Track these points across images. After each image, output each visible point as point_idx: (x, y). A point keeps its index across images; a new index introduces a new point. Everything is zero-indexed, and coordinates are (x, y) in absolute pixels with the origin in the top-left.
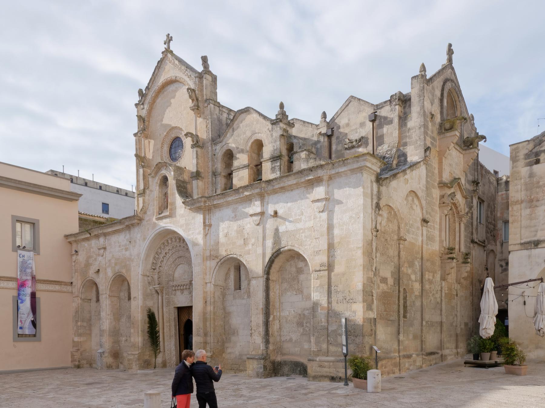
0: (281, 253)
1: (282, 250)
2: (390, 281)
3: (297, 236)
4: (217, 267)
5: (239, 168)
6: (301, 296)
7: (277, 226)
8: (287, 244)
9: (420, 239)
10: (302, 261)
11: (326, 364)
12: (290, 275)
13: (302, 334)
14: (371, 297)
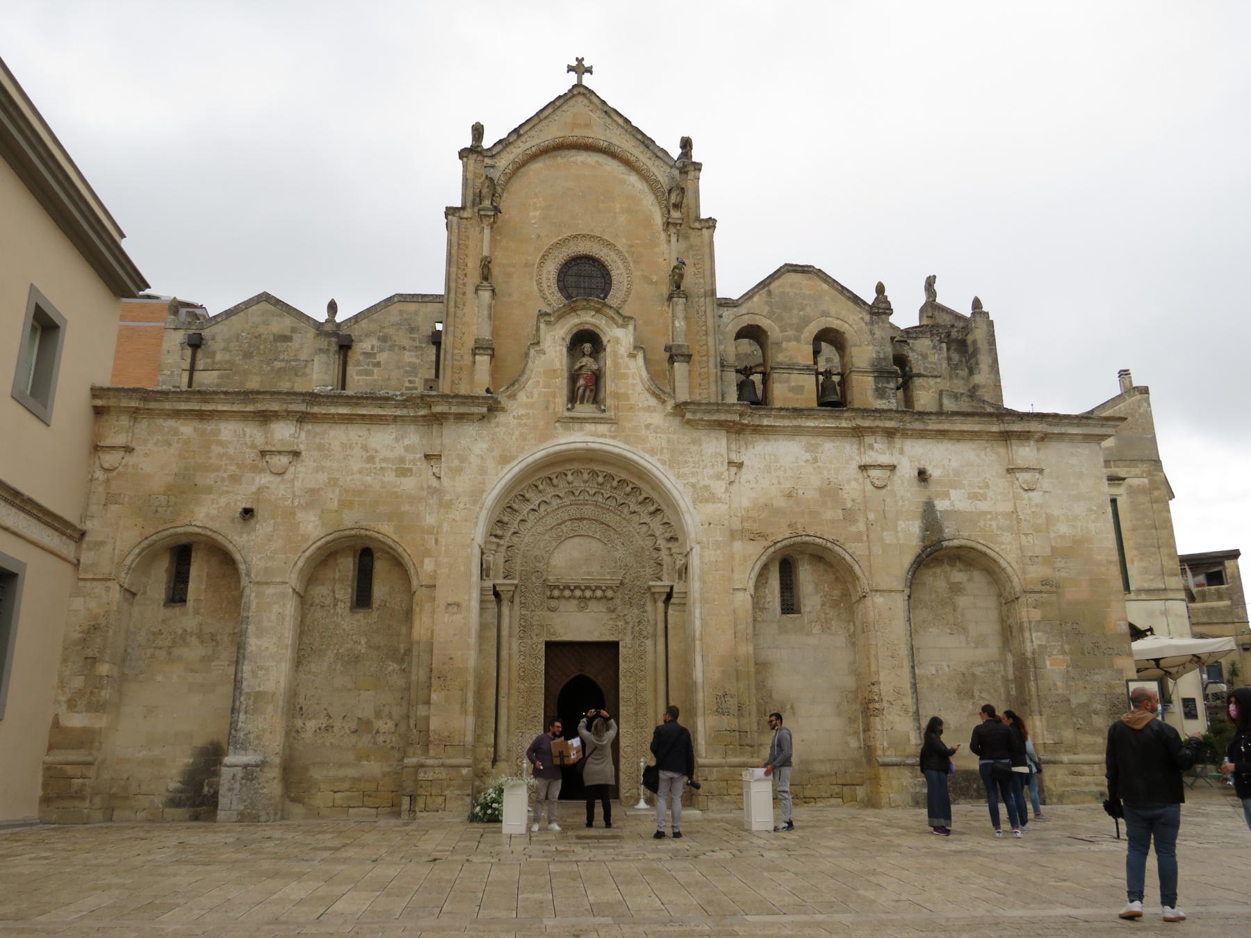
1: (945, 544)
3: (981, 524)
5: (791, 367)
8: (955, 535)
11: (1085, 767)
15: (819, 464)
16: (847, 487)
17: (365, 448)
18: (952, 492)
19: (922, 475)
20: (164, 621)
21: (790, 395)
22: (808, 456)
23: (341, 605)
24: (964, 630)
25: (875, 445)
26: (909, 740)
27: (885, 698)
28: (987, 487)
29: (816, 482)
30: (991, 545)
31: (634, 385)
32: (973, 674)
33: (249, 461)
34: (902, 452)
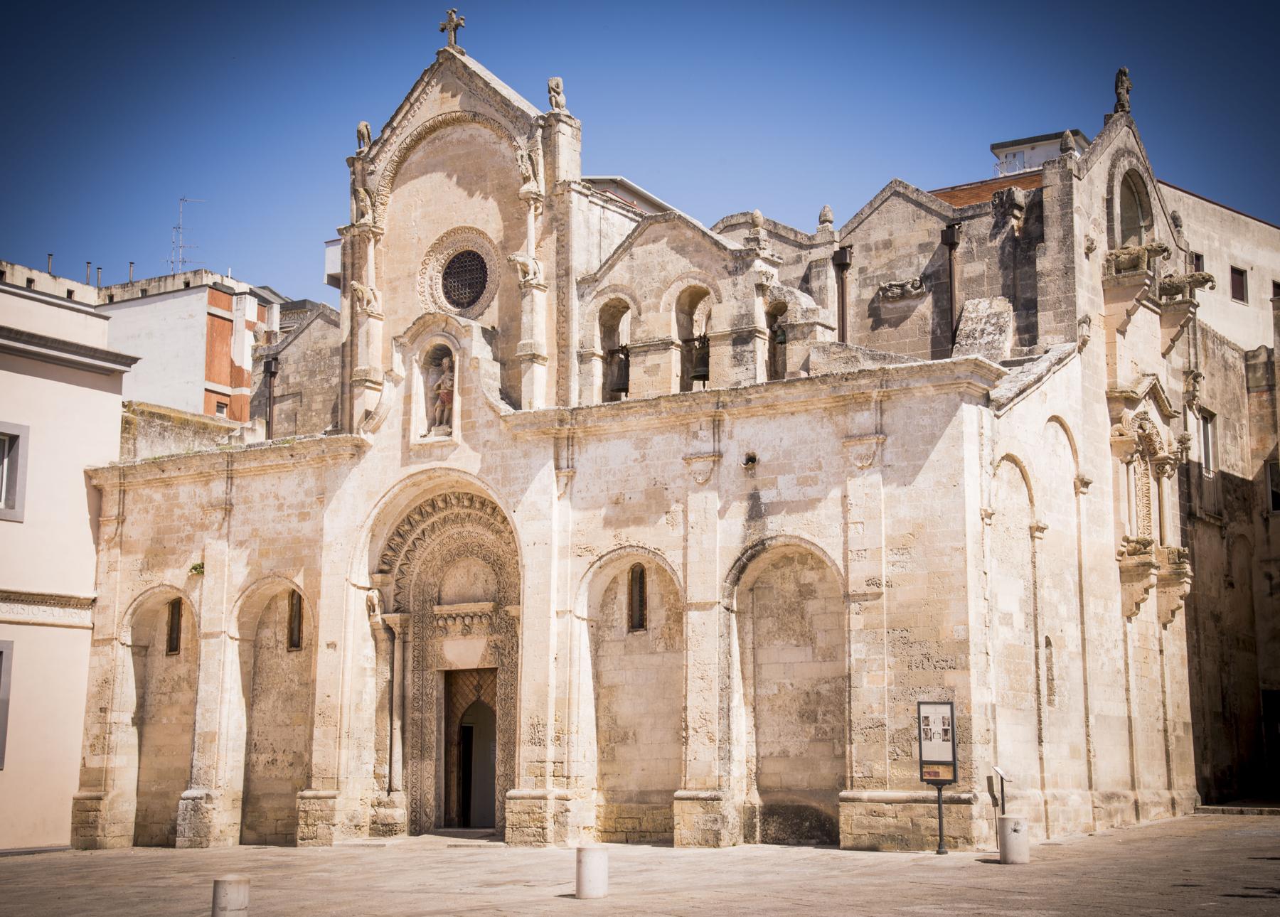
0: (764, 549)
2: (1019, 620)
4: (590, 575)
6: (809, 650)
7: (756, 489)
9: (1074, 521)
10: (812, 569)
12: (781, 601)
13: (814, 740)
14: (984, 656)
15: (648, 462)
16: (672, 485)
17: (277, 497)
18: (782, 480)
19: (751, 460)
20: (166, 670)
21: (646, 377)
22: (637, 454)
23: (281, 646)
24: (812, 640)
25: (700, 433)
26: (710, 771)
27: (691, 725)
28: (820, 468)
29: (642, 483)
30: (816, 540)
31: (476, 399)
32: (818, 693)
33: (198, 521)
34: (731, 437)
